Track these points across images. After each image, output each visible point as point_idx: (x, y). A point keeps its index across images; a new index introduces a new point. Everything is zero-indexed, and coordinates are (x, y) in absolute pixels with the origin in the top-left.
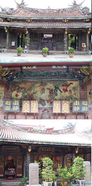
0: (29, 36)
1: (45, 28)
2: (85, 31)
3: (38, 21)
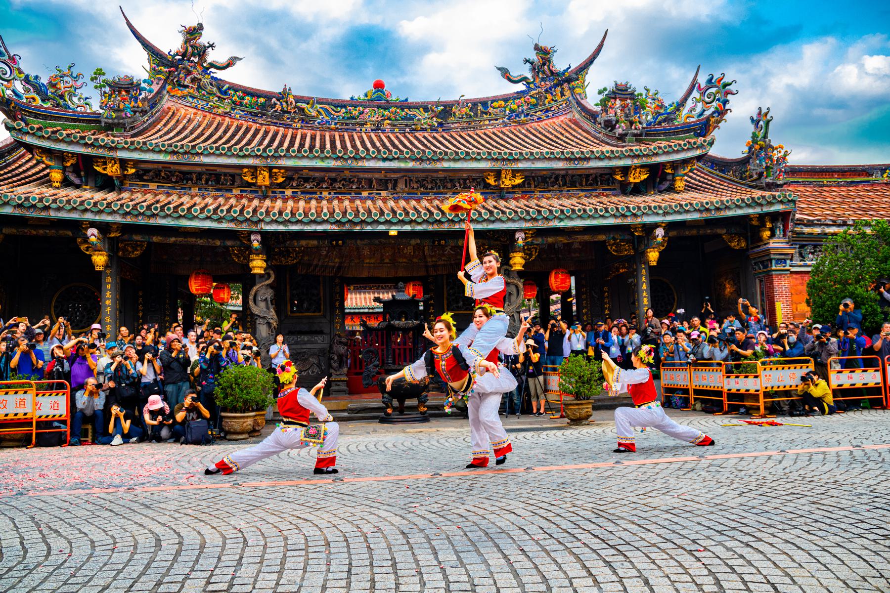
0: (269, 294)
1: (385, 234)
2: (627, 251)
3: (322, 180)
